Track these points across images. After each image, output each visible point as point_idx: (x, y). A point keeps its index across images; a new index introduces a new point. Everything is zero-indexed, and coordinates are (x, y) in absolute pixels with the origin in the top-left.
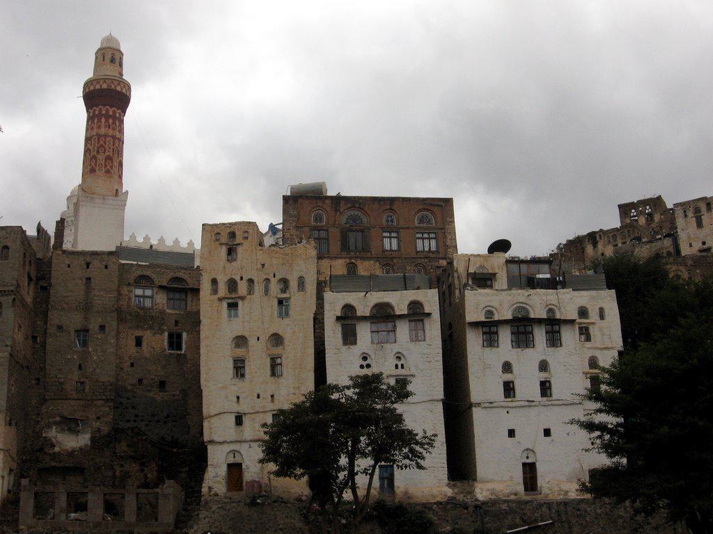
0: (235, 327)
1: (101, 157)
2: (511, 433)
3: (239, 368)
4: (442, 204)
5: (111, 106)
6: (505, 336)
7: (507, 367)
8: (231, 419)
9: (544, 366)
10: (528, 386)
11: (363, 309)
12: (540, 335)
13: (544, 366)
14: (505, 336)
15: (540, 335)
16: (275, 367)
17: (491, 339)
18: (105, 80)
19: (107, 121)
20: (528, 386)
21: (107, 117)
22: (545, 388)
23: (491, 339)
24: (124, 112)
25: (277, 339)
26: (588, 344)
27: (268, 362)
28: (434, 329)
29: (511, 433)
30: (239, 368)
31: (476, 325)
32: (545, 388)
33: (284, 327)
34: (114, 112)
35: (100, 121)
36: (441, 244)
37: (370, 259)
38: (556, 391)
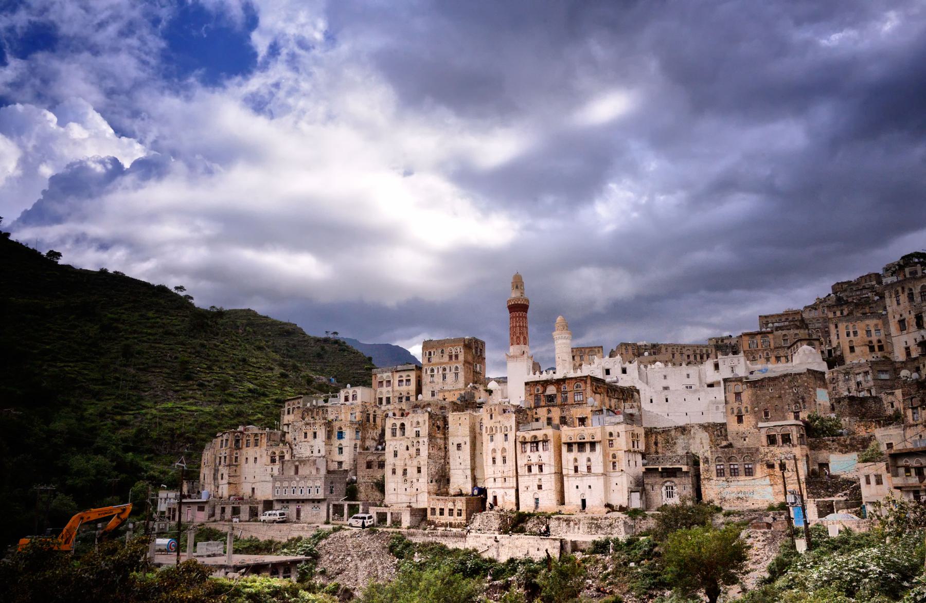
0: (491, 446)
1: (515, 338)
2: (577, 487)
3: (494, 462)
4: (585, 379)
5: (517, 311)
6: (575, 447)
7: (576, 460)
8: (493, 479)
9: (589, 460)
10: (583, 469)
11: (528, 439)
12: (588, 447)
13: (589, 460)
14: (575, 447)
15: (588, 447)
16: (504, 461)
17: (570, 449)
18: (513, 300)
19: (516, 319)
20: (583, 469)
21: (519, 317)
22: (589, 468)
23: (570, 449)
24: (526, 312)
25: (504, 450)
26: (612, 449)
27: (502, 458)
28: (551, 446)
29: (577, 487)
30: (494, 462)
31: (565, 443)
32: (589, 468)
33: (506, 445)
34: (519, 314)
35: (516, 319)
36: (584, 397)
37: (556, 406)
38: (593, 470)
